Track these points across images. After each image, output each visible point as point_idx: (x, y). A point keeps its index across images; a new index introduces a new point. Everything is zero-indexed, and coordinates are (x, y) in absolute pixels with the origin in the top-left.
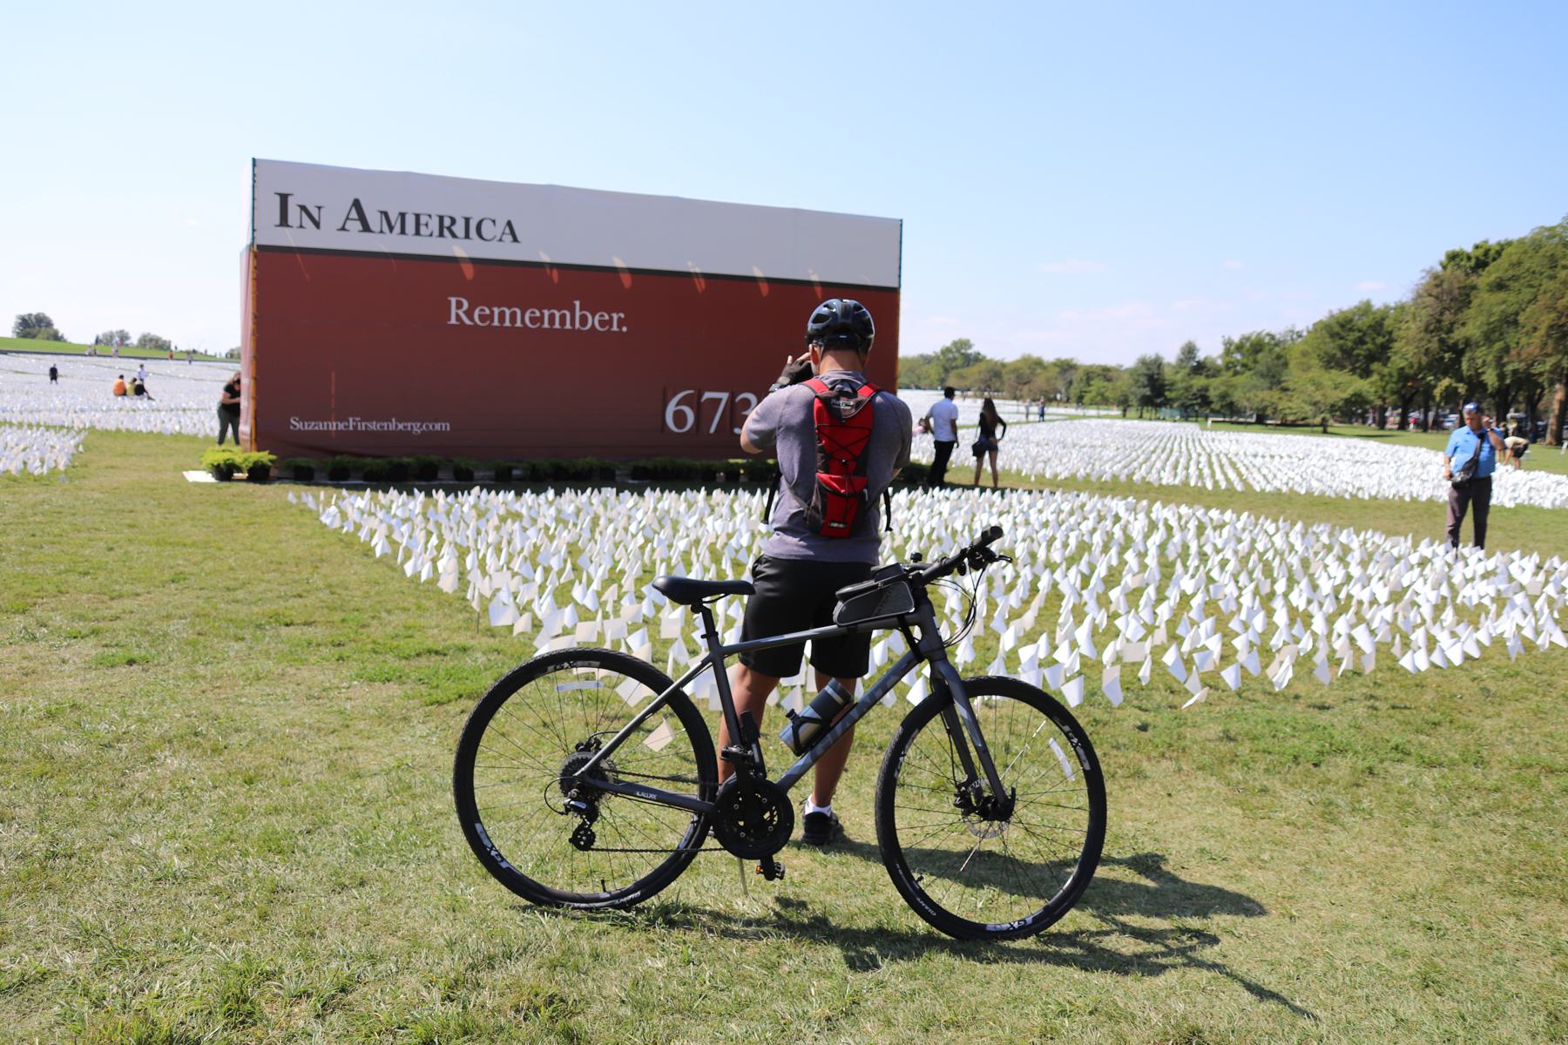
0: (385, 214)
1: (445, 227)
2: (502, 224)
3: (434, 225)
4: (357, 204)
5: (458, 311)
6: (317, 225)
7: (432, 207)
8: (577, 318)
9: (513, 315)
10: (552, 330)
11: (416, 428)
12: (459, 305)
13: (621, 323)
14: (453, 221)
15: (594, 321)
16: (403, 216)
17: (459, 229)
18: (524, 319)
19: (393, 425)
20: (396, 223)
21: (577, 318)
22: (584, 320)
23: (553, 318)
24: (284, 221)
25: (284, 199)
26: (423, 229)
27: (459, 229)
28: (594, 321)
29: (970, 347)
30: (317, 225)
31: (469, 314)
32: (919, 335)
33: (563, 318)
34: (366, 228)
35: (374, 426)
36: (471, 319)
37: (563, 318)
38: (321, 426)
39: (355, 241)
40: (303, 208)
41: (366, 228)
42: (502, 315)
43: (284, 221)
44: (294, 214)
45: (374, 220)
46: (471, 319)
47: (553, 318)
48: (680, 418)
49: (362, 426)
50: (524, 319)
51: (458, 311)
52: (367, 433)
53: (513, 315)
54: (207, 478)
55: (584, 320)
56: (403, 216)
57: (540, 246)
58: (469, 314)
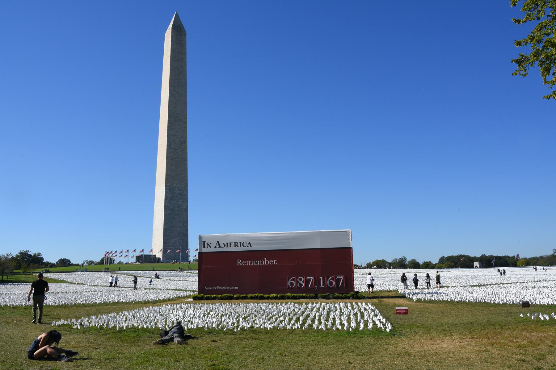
1: (236, 245)
4: (218, 242)
7: (233, 241)
8: (266, 262)
10: (260, 265)
11: (231, 288)
13: (276, 262)
15: (269, 262)
17: (239, 245)
18: (253, 263)
19: (225, 288)
21: (266, 262)
22: (267, 262)
23: (260, 263)
24: (204, 247)
25: (204, 242)
27: (239, 245)
28: (269, 262)
31: (241, 263)
35: (222, 288)
38: (211, 288)
39: (218, 250)
41: (220, 247)
45: (221, 245)
47: (260, 263)
48: (292, 284)
49: (219, 288)
50: (253, 263)
51: (239, 262)
52: (221, 290)
54: (192, 300)
55: (267, 262)
57: (254, 248)
58: (241, 263)
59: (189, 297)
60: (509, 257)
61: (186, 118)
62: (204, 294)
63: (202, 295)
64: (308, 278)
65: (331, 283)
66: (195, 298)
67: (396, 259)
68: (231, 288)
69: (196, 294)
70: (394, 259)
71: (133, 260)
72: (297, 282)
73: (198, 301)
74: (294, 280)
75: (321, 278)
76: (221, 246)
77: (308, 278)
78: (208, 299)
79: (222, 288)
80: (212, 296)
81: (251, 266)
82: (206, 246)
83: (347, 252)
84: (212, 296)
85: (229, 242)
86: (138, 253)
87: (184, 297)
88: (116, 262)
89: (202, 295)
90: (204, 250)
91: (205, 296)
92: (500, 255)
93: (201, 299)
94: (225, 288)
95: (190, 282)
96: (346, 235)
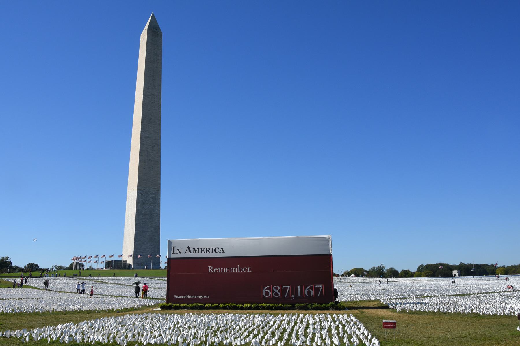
0: (194, 249)
1: (207, 251)
2: (220, 249)
3: (205, 250)
4: (188, 247)
5: (210, 269)
6: (180, 253)
7: (205, 246)
8: (239, 269)
9: (223, 270)
11: (201, 297)
12: (211, 268)
14: (209, 249)
15: (243, 270)
16: (198, 249)
17: (211, 251)
18: (226, 270)
19: (196, 297)
20: (196, 251)
22: (240, 270)
23: (233, 270)
24: (174, 253)
25: (174, 247)
26: (203, 252)
27: (211, 251)
28: (243, 270)
29: (384, 267)
30: (180, 253)
31: (213, 270)
32: (338, 267)
33: (235, 269)
34: (190, 252)
35: (192, 297)
36: (213, 270)
37: (235, 269)
38: (181, 297)
40: (178, 249)
41: (190, 252)
42: (220, 270)
43: (174, 253)
44: (176, 251)
45: (192, 251)
46: (213, 270)
47: (233, 270)
48: (267, 293)
49: (189, 297)
50: (226, 270)
51: (210, 269)
53: (223, 270)
54: (160, 309)
55: (240, 270)
56: (198, 249)
57: (227, 254)
58: (213, 270)
59: (156, 306)
60: (487, 265)
61: (160, 120)
62: (174, 303)
63: (171, 304)
64: (285, 287)
65: (309, 293)
66: (163, 307)
67: (374, 268)
68: (201, 297)
69: (165, 303)
70: (372, 267)
71: (103, 266)
72: (273, 291)
73: (166, 311)
74: (268, 289)
75: (299, 287)
76: (192, 252)
77: (285, 287)
78: (177, 308)
79: (192, 297)
80: (182, 305)
81: (223, 273)
82: (176, 252)
83: (326, 260)
84: (182, 305)
85: (200, 248)
86: (110, 259)
87: (152, 306)
88: (85, 268)
89: (171, 304)
90: (173, 256)
91: (174, 305)
92: (479, 263)
93: (170, 308)
94: (196, 297)
95: (159, 288)
96: (326, 241)
